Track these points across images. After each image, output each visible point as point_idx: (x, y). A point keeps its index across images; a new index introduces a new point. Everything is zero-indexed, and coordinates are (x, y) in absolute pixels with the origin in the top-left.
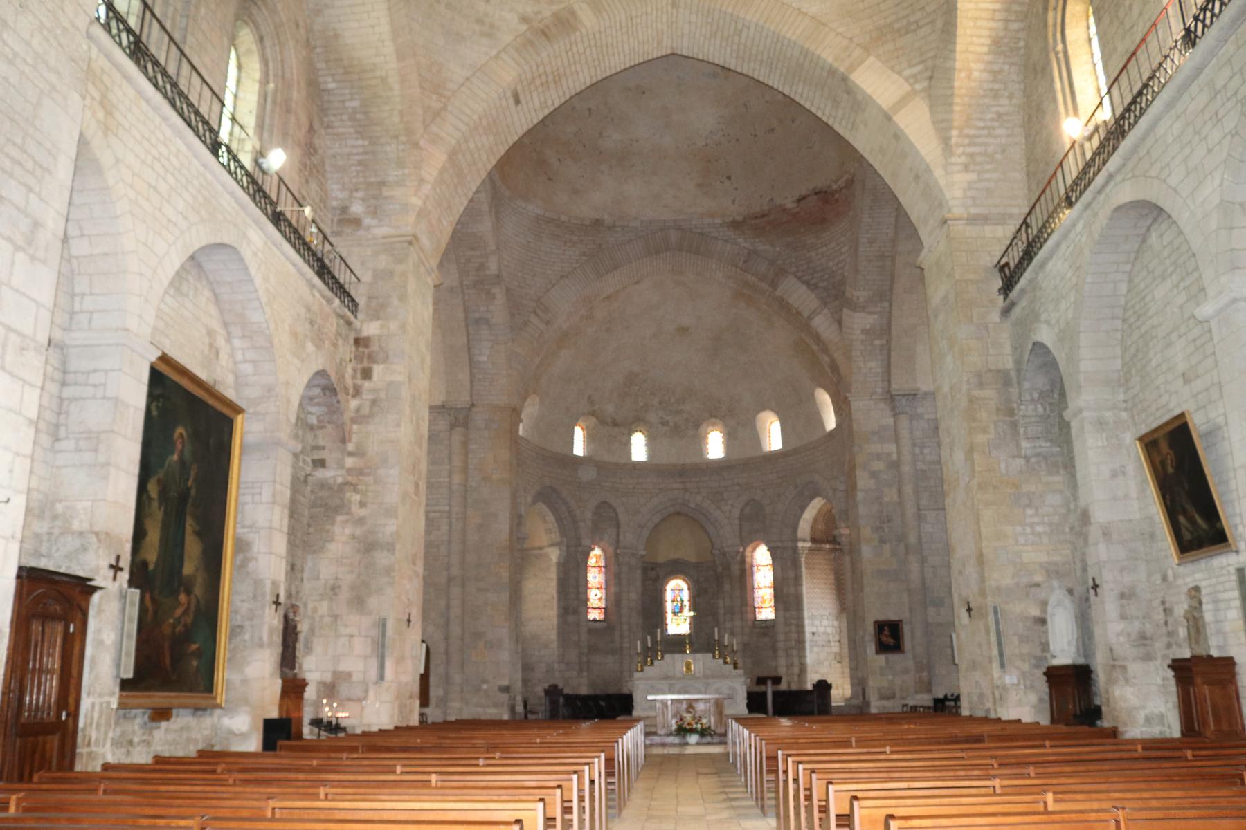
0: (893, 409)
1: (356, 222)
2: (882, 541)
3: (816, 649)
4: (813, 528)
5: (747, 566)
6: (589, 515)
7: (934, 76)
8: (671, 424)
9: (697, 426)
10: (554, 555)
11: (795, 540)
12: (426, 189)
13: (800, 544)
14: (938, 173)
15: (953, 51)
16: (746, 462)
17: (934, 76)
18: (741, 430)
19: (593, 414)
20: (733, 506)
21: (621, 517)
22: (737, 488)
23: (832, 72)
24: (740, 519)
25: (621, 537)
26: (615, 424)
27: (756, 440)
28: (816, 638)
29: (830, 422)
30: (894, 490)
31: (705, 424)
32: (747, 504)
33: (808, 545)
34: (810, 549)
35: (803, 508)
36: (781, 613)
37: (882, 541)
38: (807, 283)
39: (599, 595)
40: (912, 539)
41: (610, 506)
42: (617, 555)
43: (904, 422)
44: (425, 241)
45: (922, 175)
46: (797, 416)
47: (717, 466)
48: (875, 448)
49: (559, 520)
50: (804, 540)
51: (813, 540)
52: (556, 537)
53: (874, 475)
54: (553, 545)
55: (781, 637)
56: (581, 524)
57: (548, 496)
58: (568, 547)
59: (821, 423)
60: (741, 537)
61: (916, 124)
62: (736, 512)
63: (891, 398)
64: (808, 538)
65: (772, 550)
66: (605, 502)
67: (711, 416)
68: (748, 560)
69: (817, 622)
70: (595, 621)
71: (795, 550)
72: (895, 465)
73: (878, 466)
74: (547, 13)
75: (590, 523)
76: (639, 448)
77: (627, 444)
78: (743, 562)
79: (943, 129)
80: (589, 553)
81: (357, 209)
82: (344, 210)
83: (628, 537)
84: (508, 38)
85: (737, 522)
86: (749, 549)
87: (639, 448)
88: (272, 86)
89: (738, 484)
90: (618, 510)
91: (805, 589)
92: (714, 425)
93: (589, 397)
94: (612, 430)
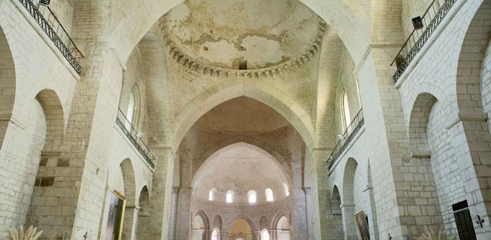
0: (305, 192)
1: (155, 142)
2: (301, 232)
6: (213, 219)
7: (312, 110)
9: (247, 192)
10: (202, 232)
11: (276, 229)
12: (175, 134)
14: (313, 136)
15: (317, 104)
16: (262, 204)
17: (312, 110)
18: (261, 195)
21: (223, 221)
23: (285, 106)
24: (260, 222)
26: (222, 191)
27: (265, 197)
30: (305, 217)
35: (279, 219)
37: (301, 232)
38: (281, 154)
40: (310, 232)
43: (308, 196)
44: (173, 148)
45: (308, 134)
46: (277, 189)
48: (300, 204)
49: (204, 220)
52: (202, 226)
53: (299, 212)
56: (210, 222)
57: (202, 213)
59: (285, 193)
61: (306, 121)
62: (259, 220)
63: (303, 189)
65: (269, 232)
72: (306, 209)
73: (300, 209)
74: (209, 86)
77: (225, 197)
78: (260, 236)
79: (314, 123)
81: (155, 138)
82: (152, 138)
83: (224, 227)
84: (198, 93)
88: (136, 108)
94: (221, 192)
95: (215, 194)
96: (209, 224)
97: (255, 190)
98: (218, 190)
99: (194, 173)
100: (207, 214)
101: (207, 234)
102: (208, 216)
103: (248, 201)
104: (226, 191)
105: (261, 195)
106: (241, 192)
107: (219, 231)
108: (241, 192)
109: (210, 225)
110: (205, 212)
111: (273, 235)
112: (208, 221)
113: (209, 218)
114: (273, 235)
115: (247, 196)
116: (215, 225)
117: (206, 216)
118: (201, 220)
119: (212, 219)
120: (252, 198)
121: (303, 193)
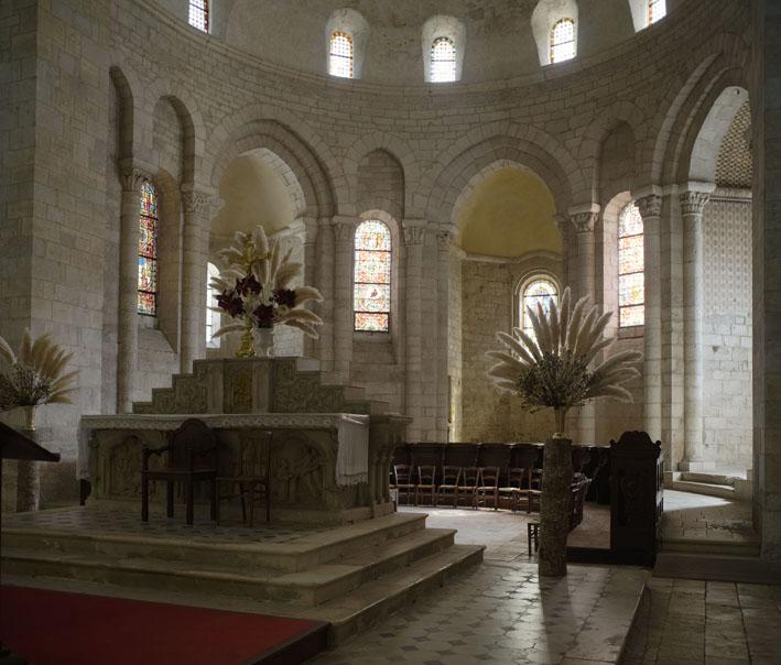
3: (717, 375)
4: (723, 159)
5: (607, 237)
6: (351, 167)
13: (693, 188)
20: (584, 138)
21: (406, 173)
22: (593, 105)
25: (408, 203)
26: (395, 23)
28: (717, 356)
32: (611, 132)
33: (710, 189)
34: (714, 199)
36: (657, 311)
39: (379, 295)
41: (392, 156)
42: (402, 229)
50: (702, 181)
51: (721, 184)
52: (301, 204)
54: (298, 217)
55: (656, 353)
58: (319, 217)
60: (600, 191)
62: (593, 148)
64: (712, 177)
65: (644, 206)
66: (382, 150)
68: (609, 228)
69: (724, 329)
70: (371, 332)
71: (685, 197)
75: (353, 181)
76: (443, 65)
78: (599, 230)
80: (352, 229)
85: (594, 163)
86: (611, 208)
87: (443, 65)
89: (595, 100)
90: (404, 161)
91: (700, 269)
94: (391, 42)
95: (365, 50)
96: (330, 190)
98: (372, 20)
101: (326, 239)
102: (324, 155)
103: (534, 55)
107: (394, 223)
109: (340, 194)
111: (664, 216)
112: (327, 180)
113: (331, 164)
114: (664, 216)
116: (366, 204)
117: (311, 150)
118: (291, 176)
119: (347, 168)
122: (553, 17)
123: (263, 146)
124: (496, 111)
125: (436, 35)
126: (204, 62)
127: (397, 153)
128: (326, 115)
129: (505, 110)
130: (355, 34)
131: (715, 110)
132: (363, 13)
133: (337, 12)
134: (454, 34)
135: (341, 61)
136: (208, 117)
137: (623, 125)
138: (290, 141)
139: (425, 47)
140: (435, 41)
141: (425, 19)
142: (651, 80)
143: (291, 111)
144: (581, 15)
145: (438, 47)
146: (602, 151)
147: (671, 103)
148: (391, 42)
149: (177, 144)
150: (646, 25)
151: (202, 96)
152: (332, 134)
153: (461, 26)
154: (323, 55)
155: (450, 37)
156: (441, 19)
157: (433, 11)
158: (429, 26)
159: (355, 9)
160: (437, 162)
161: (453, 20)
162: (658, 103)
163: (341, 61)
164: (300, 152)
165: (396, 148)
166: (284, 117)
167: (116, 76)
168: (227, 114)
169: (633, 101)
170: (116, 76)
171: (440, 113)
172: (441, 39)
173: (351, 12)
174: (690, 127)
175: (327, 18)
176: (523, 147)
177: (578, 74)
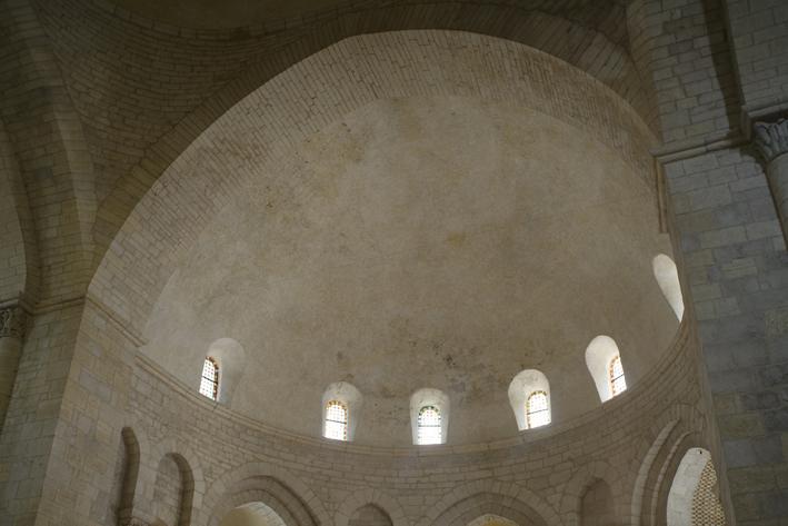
8: (469, 388)
9: (505, 384)
18: (572, 385)
19: (349, 379)
20: (564, 494)
22: (570, 464)
29: (679, 309)
31: (516, 379)
46: (627, 313)
47: (539, 442)
62: (574, 503)
67: (523, 367)
76: (430, 430)
87: (430, 430)
89: (570, 459)
92: (531, 381)
93: (340, 356)
94: (384, 410)
95: (357, 415)
97: (539, 366)
98: (364, 392)
99: (106, 229)
100: (306, 498)
104: (407, 394)
105: (572, 385)
106: (481, 398)
108: (481, 398)
110: (300, 487)
115: (506, 400)
117: (304, 505)
120: (535, 409)
121: (749, 164)
122: (528, 391)
123: (260, 500)
124: (480, 469)
125: (424, 404)
126: (210, 424)
127: (386, 508)
128: (320, 473)
129: (488, 469)
130: (349, 403)
131: (682, 468)
132: (357, 386)
133: (333, 385)
134: (439, 404)
135: (336, 426)
136: (208, 473)
137: (599, 481)
138: (285, 497)
139: (413, 415)
140: (422, 410)
141: (413, 391)
142: (621, 442)
143: (288, 469)
144: (552, 388)
145: (425, 414)
146: (582, 505)
147: (641, 462)
148: (384, 410)
149: (177, 497)
150: (610, 397)
151: (205, 454)
152: (325, 490)
153: (445, 397)
154: (319, 420)
155: (436, 406)
156: (428, 392)
157: (420, 385)
158: (417, 397)
159: (350, 382)
160: (424, 516)
161: (438, 393)
162: (630, 462)
163: (336, 426)
164: (294, 506)
165: (382, 504)
166: (281, 475)
167: (128, 437)
168: (226, 471)
169: (606, 460)
170: (128, 437)
171: (427, 471)
172: (427, 407)
173: (346, 385)
174: (662, 483)
175: (324, 390)
176: (506, 503)
177: (553, 438)
